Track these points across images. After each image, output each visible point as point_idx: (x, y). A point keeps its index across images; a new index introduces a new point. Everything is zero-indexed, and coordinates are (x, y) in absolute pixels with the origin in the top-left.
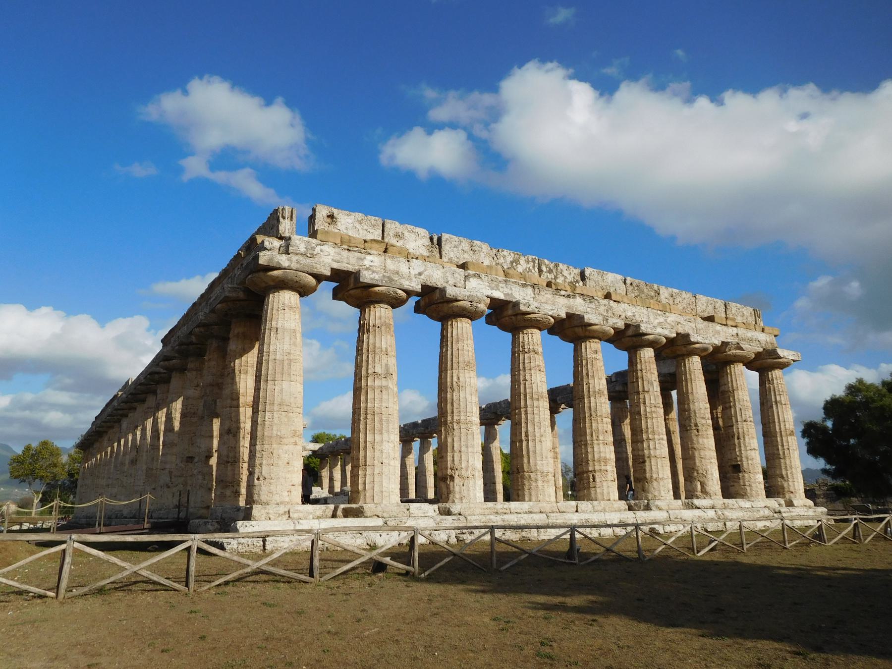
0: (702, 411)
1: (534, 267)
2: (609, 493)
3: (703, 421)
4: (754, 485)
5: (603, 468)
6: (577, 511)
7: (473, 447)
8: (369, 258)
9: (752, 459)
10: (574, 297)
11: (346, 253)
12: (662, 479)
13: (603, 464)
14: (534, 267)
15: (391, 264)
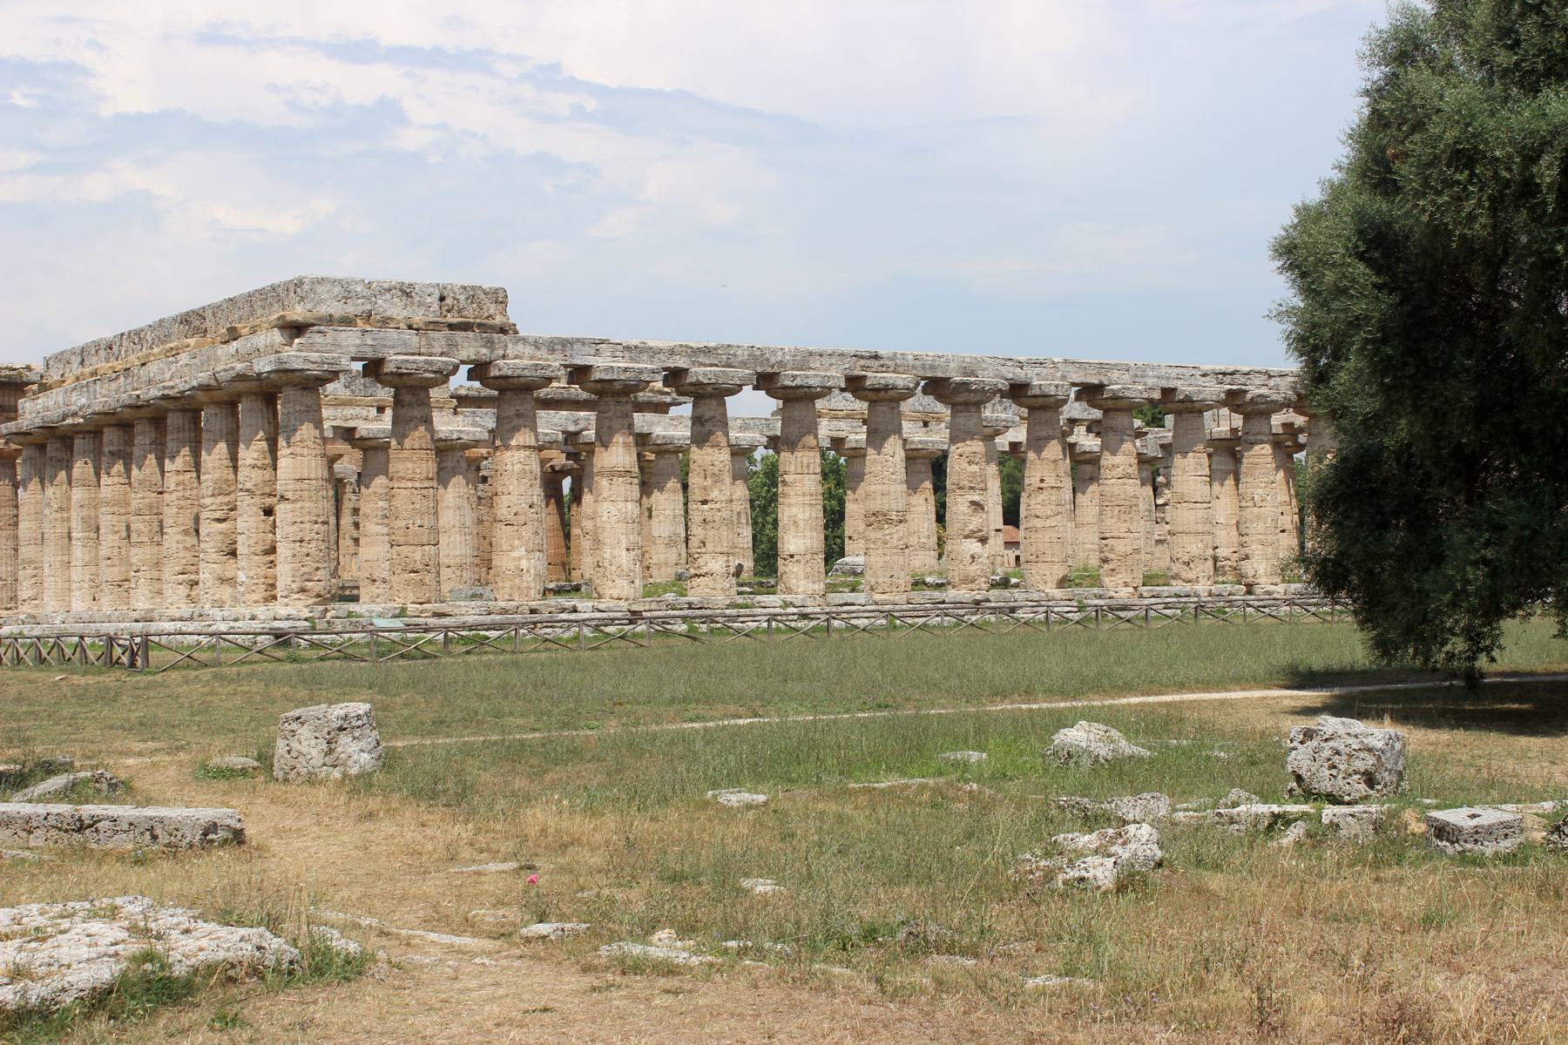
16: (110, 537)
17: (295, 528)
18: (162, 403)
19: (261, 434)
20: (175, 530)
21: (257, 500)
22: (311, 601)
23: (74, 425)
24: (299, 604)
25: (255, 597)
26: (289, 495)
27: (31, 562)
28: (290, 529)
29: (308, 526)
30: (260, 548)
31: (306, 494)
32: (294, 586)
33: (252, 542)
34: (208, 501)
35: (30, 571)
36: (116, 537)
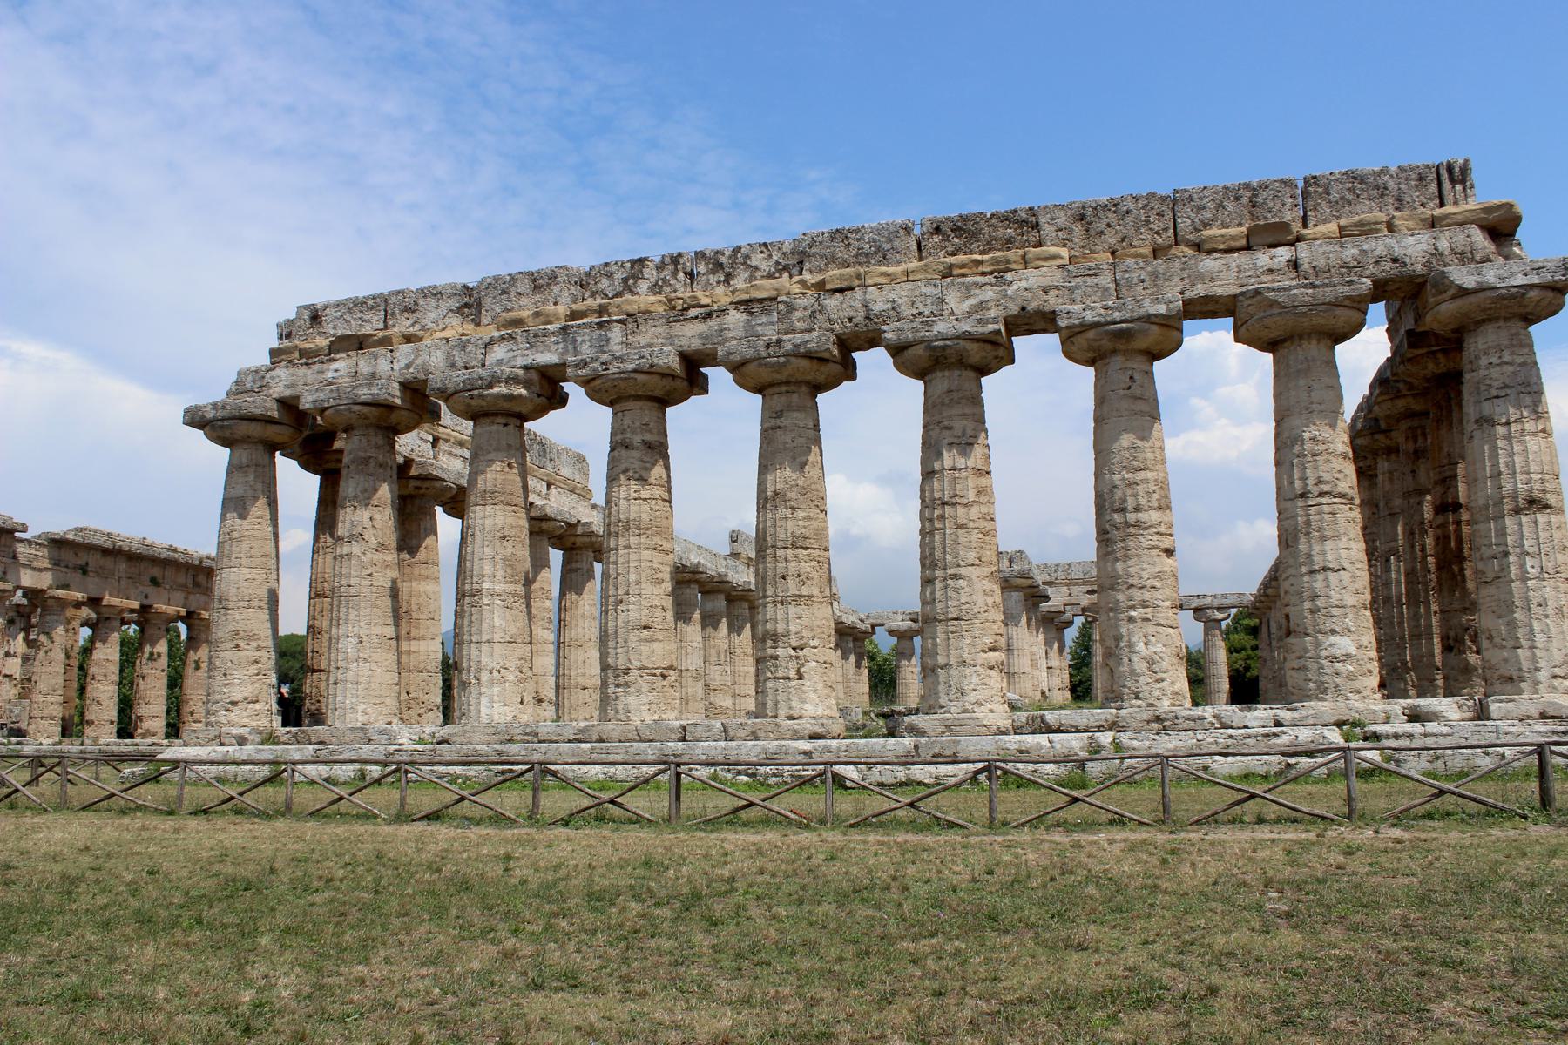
0: (1119, 494)
1: (675, 274)
2: (776, 703)
3: (1117, 517)
4: (1312, 666)
5: (770, 651)
6: (684, 739)
7: (480, 632)
8: (335, 365)
9: (1314, 597)
10: (723, 312)
11: (303, 371)
12: (946, 666)
13: (769, 643)
14: (675, 274)
15: (365, 366)
16: (648, 589)
23: (510, 398)
27: (250, 637)
35: (248, 653)
36: (658, 590)
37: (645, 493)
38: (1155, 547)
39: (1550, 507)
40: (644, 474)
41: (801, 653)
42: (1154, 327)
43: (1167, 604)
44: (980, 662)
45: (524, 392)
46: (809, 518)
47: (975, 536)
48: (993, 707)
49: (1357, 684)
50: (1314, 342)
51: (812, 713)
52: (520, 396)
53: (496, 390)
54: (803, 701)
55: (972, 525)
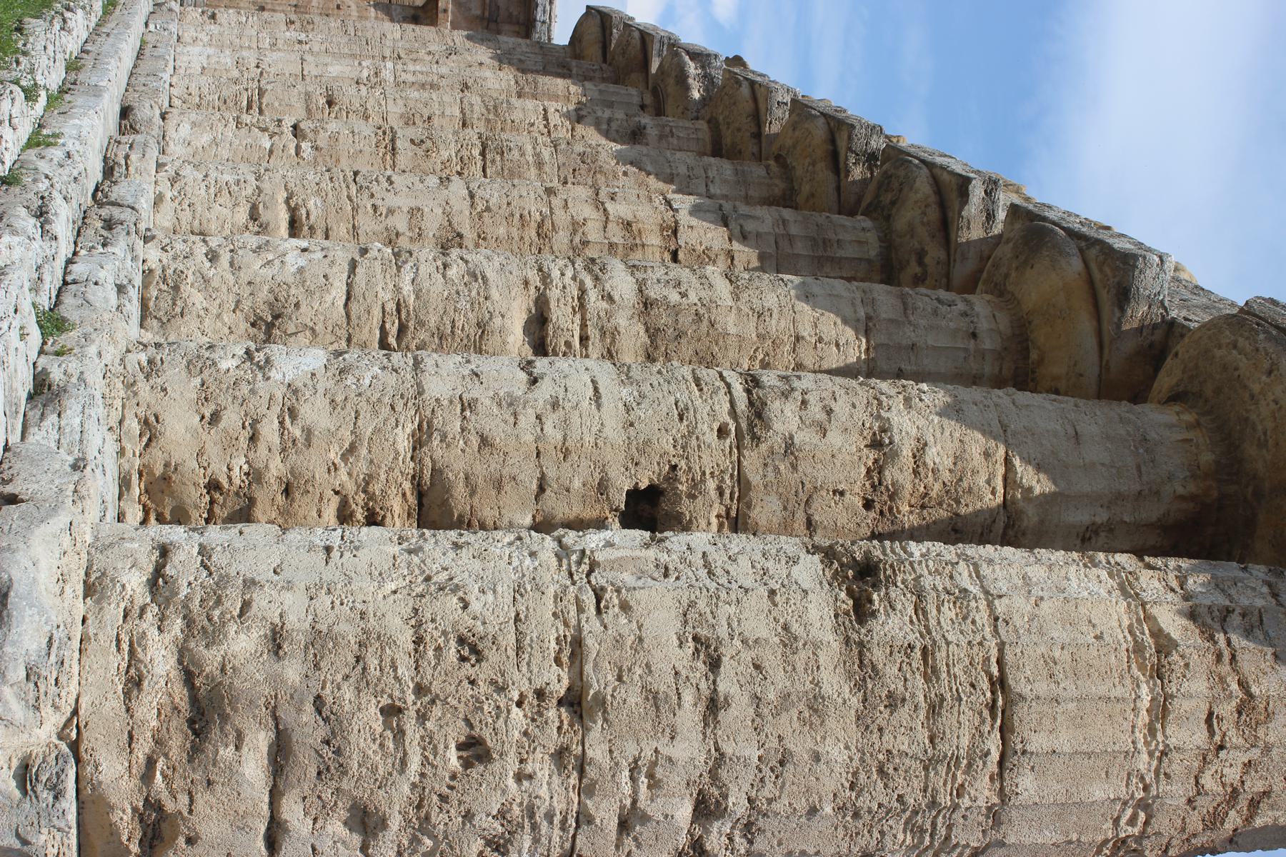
17: (672, 657)
18: (923, 186)
19: (1037, 483)
20: (460, 205)
21: (713, 456)
22: (114, 773)
24: (94, 684)
25: (180, 426)
26: (893, 624)
28: (660, 612)
29: (688, 750)
30: (456, 459)
31: (905, 733)
32: (243, 644)
33: (492, 421)
34: (622, 283)
37: (555, 119)
38: (546, 278)
39: (862, 611)
40: (588, 120)
41: (287, 130)
42: (1076, 264)
43: (407, 289)
44: (266, 186)
45: (696, 95)
46: (540, 165)
47: (534, 207)
48: (168, 206)
49: (174, 374)
50: (1188, 417)
51: (171, 133)
52: (687, 88)
53: (692, 64)
54: (194, 124)
55: (557, 202)
